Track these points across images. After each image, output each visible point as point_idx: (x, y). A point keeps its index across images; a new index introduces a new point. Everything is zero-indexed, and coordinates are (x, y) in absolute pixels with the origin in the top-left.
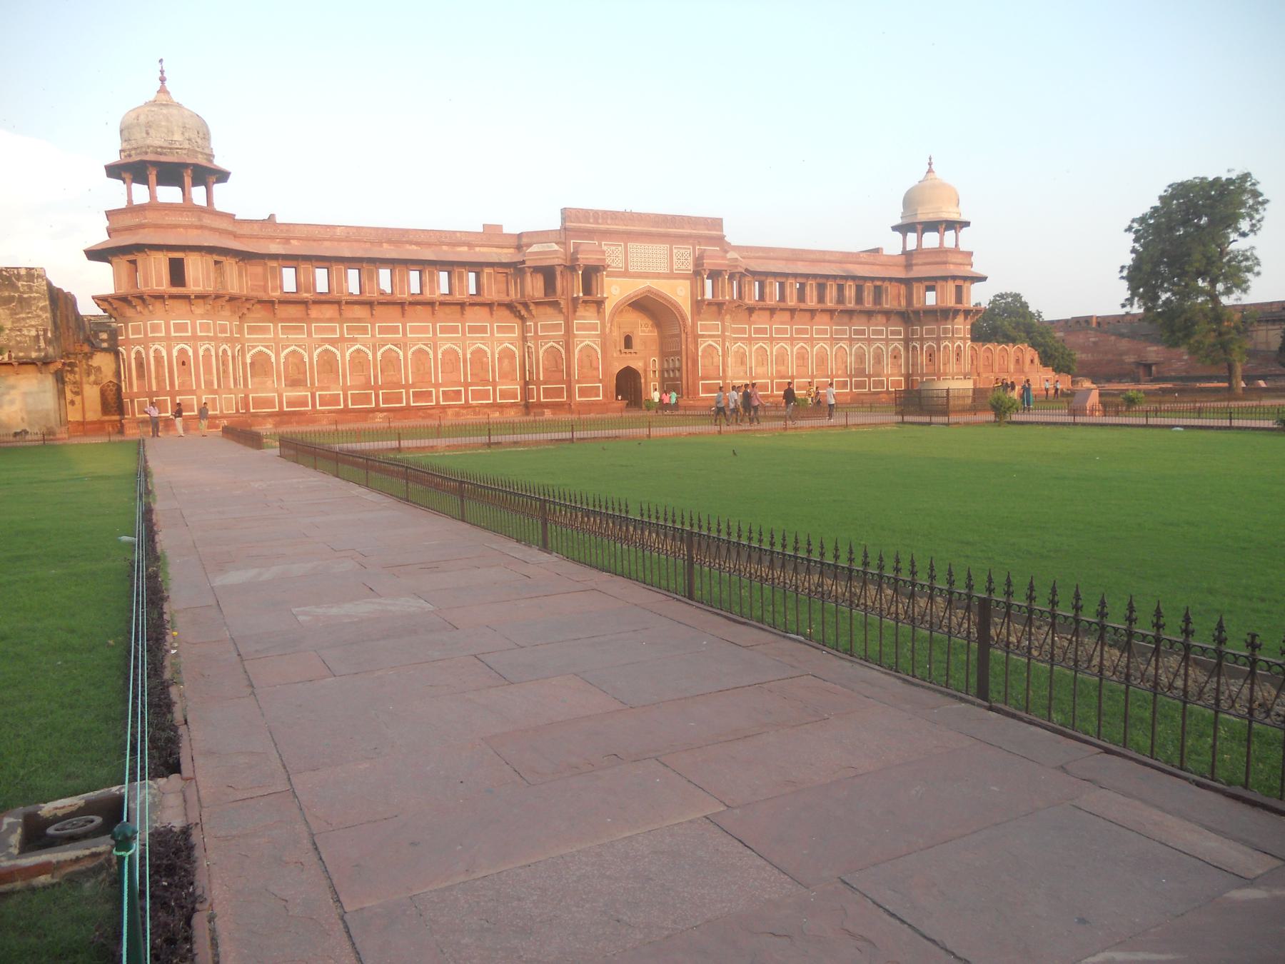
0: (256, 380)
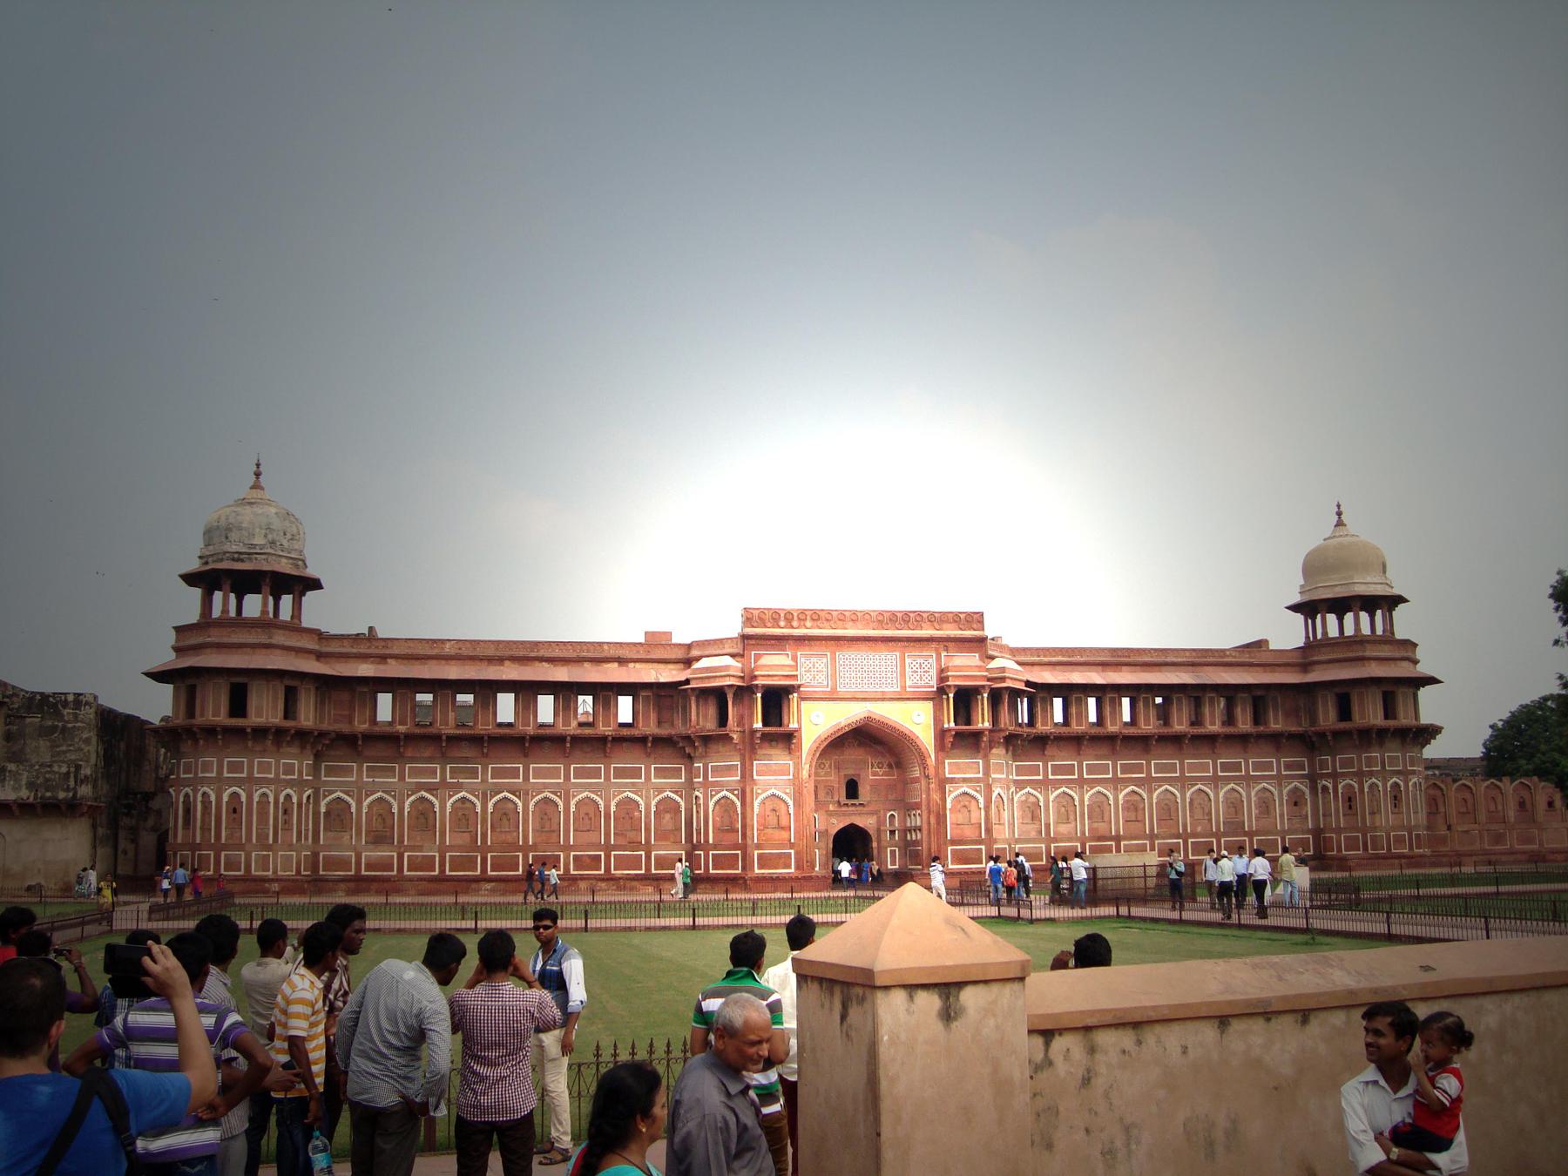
0: (330, 834)
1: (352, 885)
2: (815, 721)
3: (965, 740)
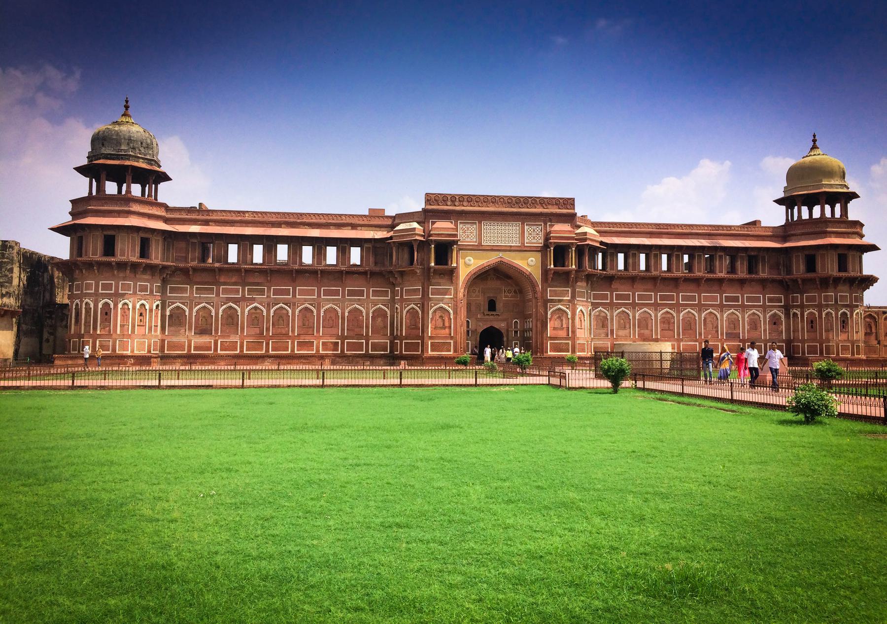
0: (172, 328)
1: (185, 360)
2: (467, 265)
3: (562, 278)
